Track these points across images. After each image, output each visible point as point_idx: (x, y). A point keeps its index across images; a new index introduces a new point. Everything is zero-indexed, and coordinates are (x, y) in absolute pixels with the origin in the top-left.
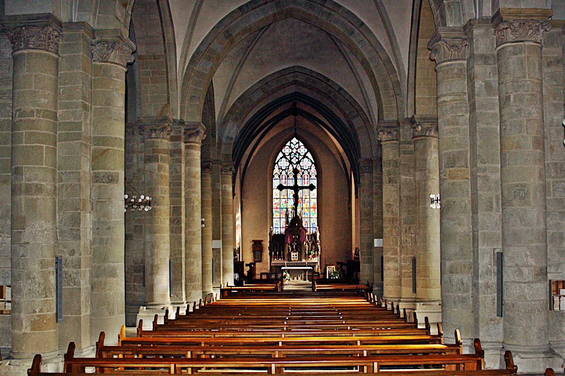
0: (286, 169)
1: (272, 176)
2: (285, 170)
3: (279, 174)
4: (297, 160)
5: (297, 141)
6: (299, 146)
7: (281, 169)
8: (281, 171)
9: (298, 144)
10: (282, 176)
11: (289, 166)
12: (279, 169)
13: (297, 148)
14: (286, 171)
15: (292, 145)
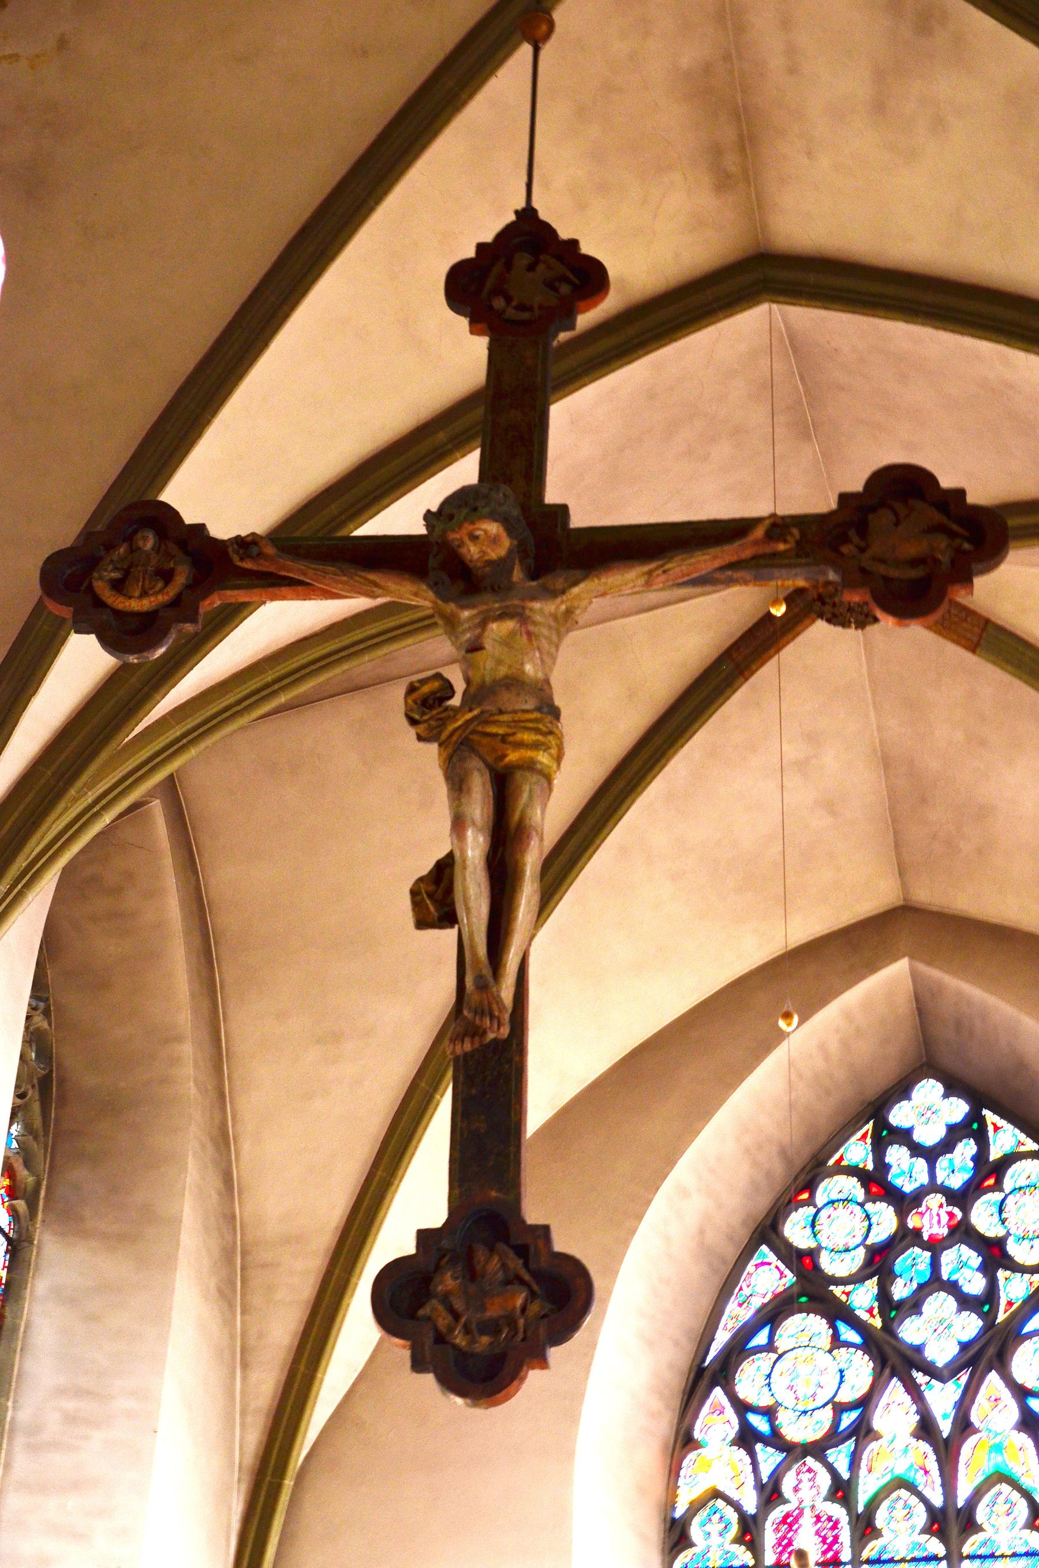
0: (833, 1437)
1: (653, 1531)
2: (818, 1449)
3: (750, 1506)
4: (970, 1325)
5: (958, 1109)
6: (980, 1158)
7: (776, 1440)
8: (769, 1458)
9: (967, 1148)
10: (790, 1521)
11: (866, 1403)
12: (746, 1438)
13: (956, 1182)
14: (840, 1457)
15: (897, 1155)
